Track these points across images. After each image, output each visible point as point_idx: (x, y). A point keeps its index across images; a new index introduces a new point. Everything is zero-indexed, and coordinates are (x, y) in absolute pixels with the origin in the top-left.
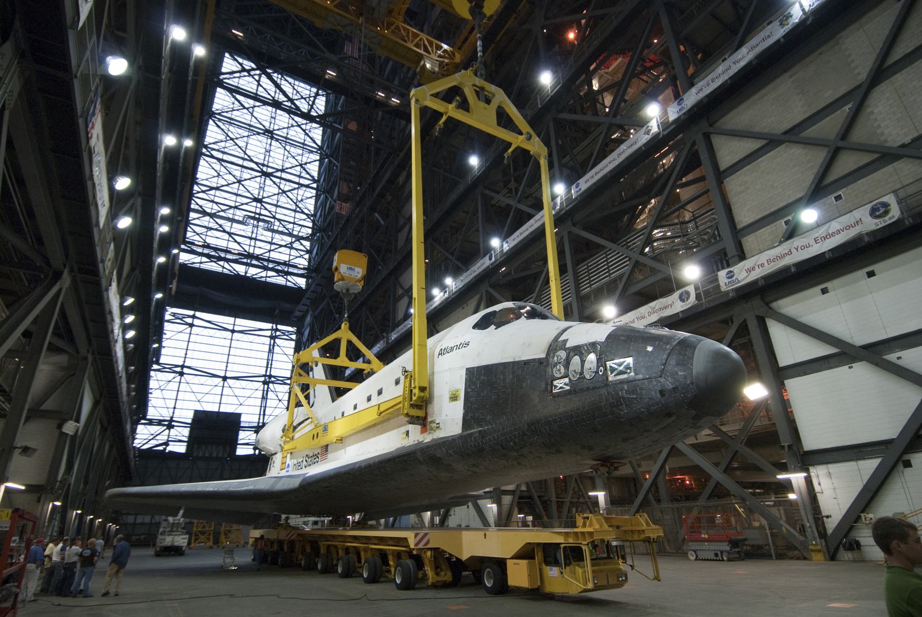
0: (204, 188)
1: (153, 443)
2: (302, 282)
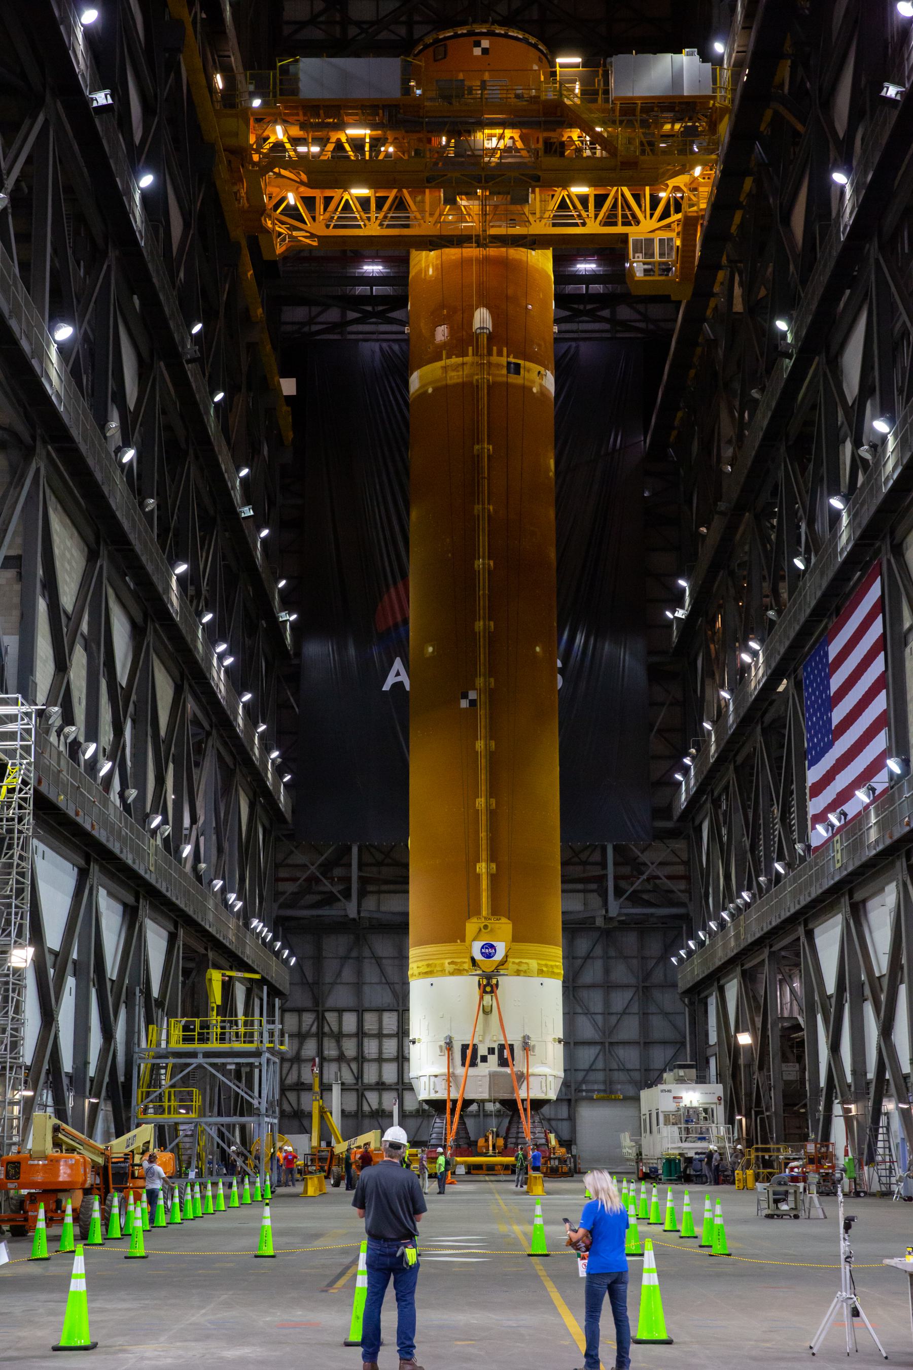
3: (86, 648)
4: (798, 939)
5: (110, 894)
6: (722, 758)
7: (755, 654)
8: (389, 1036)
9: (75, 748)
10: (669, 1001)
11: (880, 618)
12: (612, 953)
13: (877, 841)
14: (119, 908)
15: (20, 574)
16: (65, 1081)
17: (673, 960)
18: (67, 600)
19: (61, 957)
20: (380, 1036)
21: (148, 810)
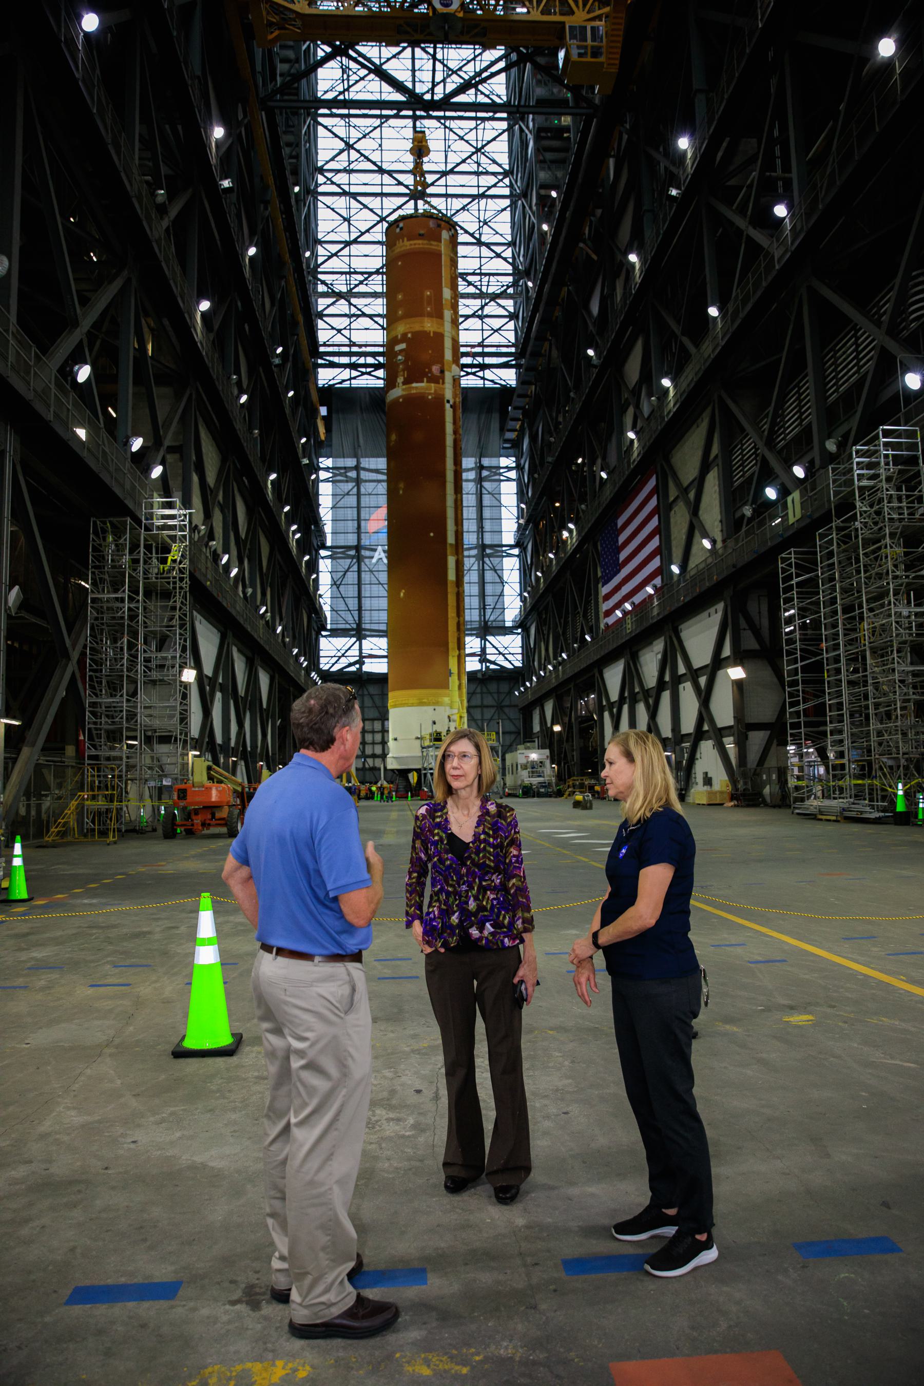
0: (334, 248)
1: (344, 662)
2: (509, 377)
3: (222, 511)
4: (594, 675)
5: (239, 651)
6: (547, 590)
7: (570, 531)
8: (378, 732)
9: (216, 557)
10: (514, 714)
11: (655, 497)
12: (485, 690)
13: (658, 614)
14: (244, 659)
15: (182, 456)
16: (218, 748)
17: (517, 693)
18: (211, 479)
19: (212, 680)
20: (373, 732)
21: (258, 603)
